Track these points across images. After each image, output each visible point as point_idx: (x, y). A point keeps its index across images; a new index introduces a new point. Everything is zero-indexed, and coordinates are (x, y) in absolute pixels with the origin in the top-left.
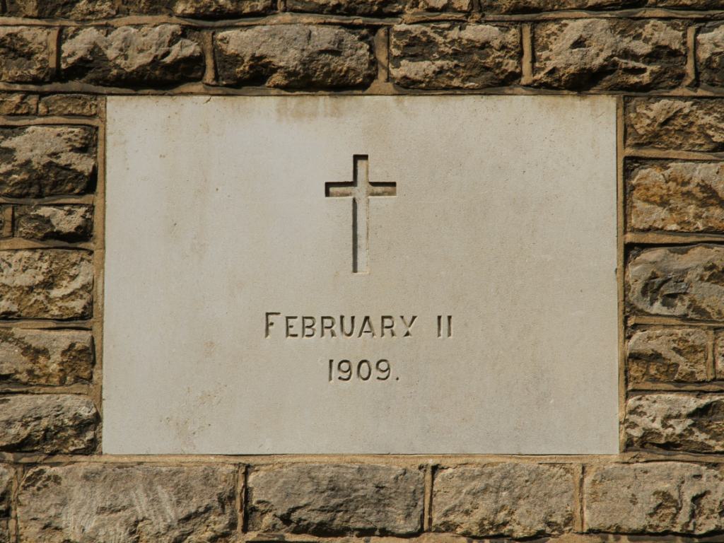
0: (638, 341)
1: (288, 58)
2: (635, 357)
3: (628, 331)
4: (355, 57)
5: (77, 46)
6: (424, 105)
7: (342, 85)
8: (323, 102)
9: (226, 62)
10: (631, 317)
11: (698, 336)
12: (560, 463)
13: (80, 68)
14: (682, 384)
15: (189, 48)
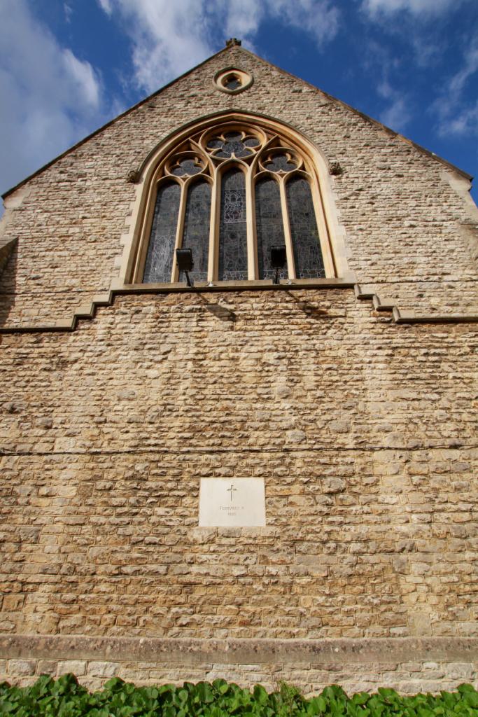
0: (268, 510)
1: (223, 473)
2: (267, 512)
3: (267, 508)
4: (231, 473)
5: (197, 472)
6: (240, 479)
7: (230, 476)
8: (227, 479)
9: (215, 473)
10: (266, 506)
11: (275, 509)
12: (258, 527)
13: (198, 474)
14: (273, 516)
15: (211, 472)
